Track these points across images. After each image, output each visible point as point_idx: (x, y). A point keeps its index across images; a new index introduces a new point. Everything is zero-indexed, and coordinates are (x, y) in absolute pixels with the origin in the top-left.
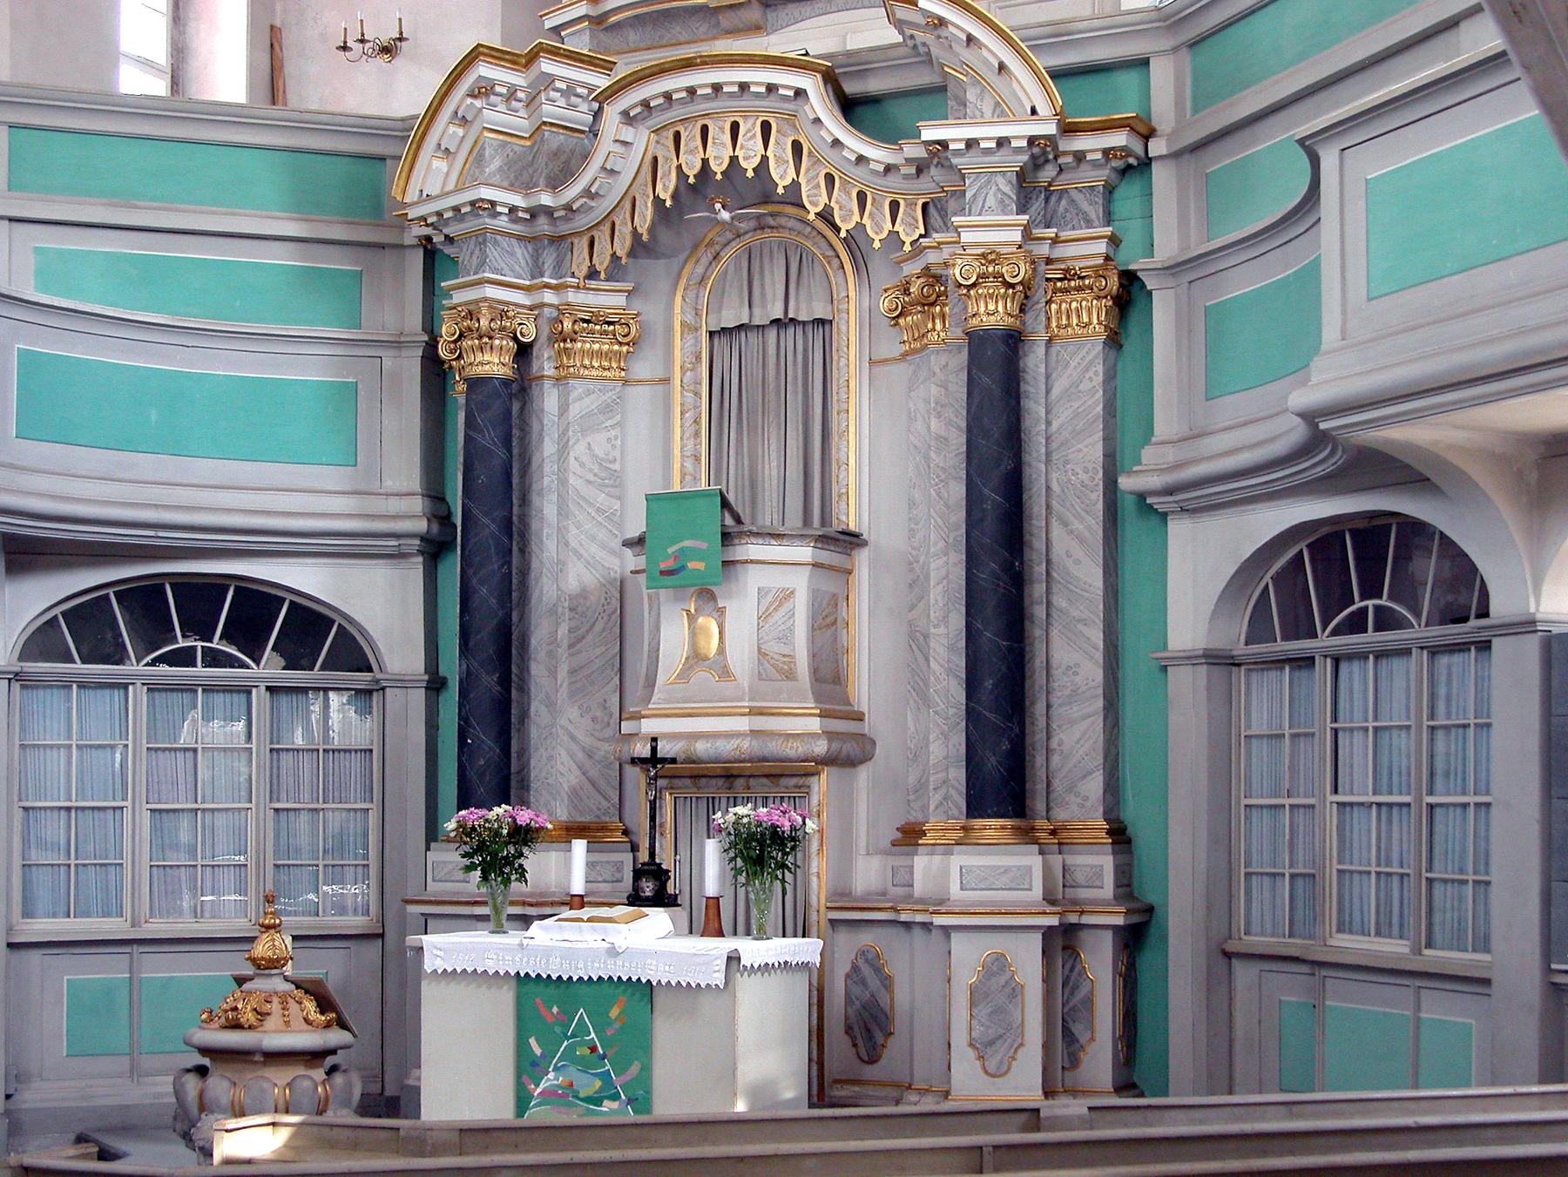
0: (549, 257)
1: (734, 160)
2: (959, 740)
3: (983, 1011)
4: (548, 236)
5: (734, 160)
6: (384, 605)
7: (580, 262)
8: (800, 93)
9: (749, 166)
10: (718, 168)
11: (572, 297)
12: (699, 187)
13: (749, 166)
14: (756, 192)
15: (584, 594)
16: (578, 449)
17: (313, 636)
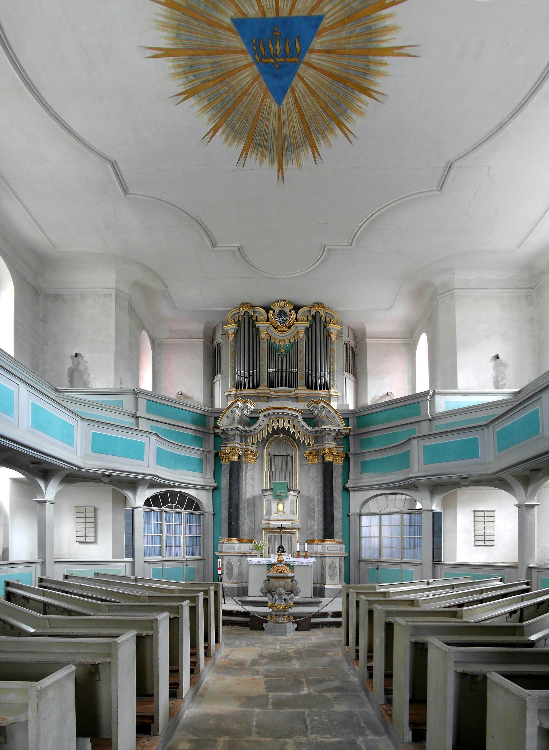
0: (244, 439)
1: (284, 426)
2: (321, 527)
3: (331, 570)
4: (244, 437)
5: (284, 426)
6: (204, 499)
7: (250, 442)
8: (297, 416)
9: (286, 428)
10: (281, 428)
11: (249, 447)
12: (276, 431)
13: (286, 428)
14: (286, 432)
15: (249, 499)
16: (248, 473)
17: (192, 504)
